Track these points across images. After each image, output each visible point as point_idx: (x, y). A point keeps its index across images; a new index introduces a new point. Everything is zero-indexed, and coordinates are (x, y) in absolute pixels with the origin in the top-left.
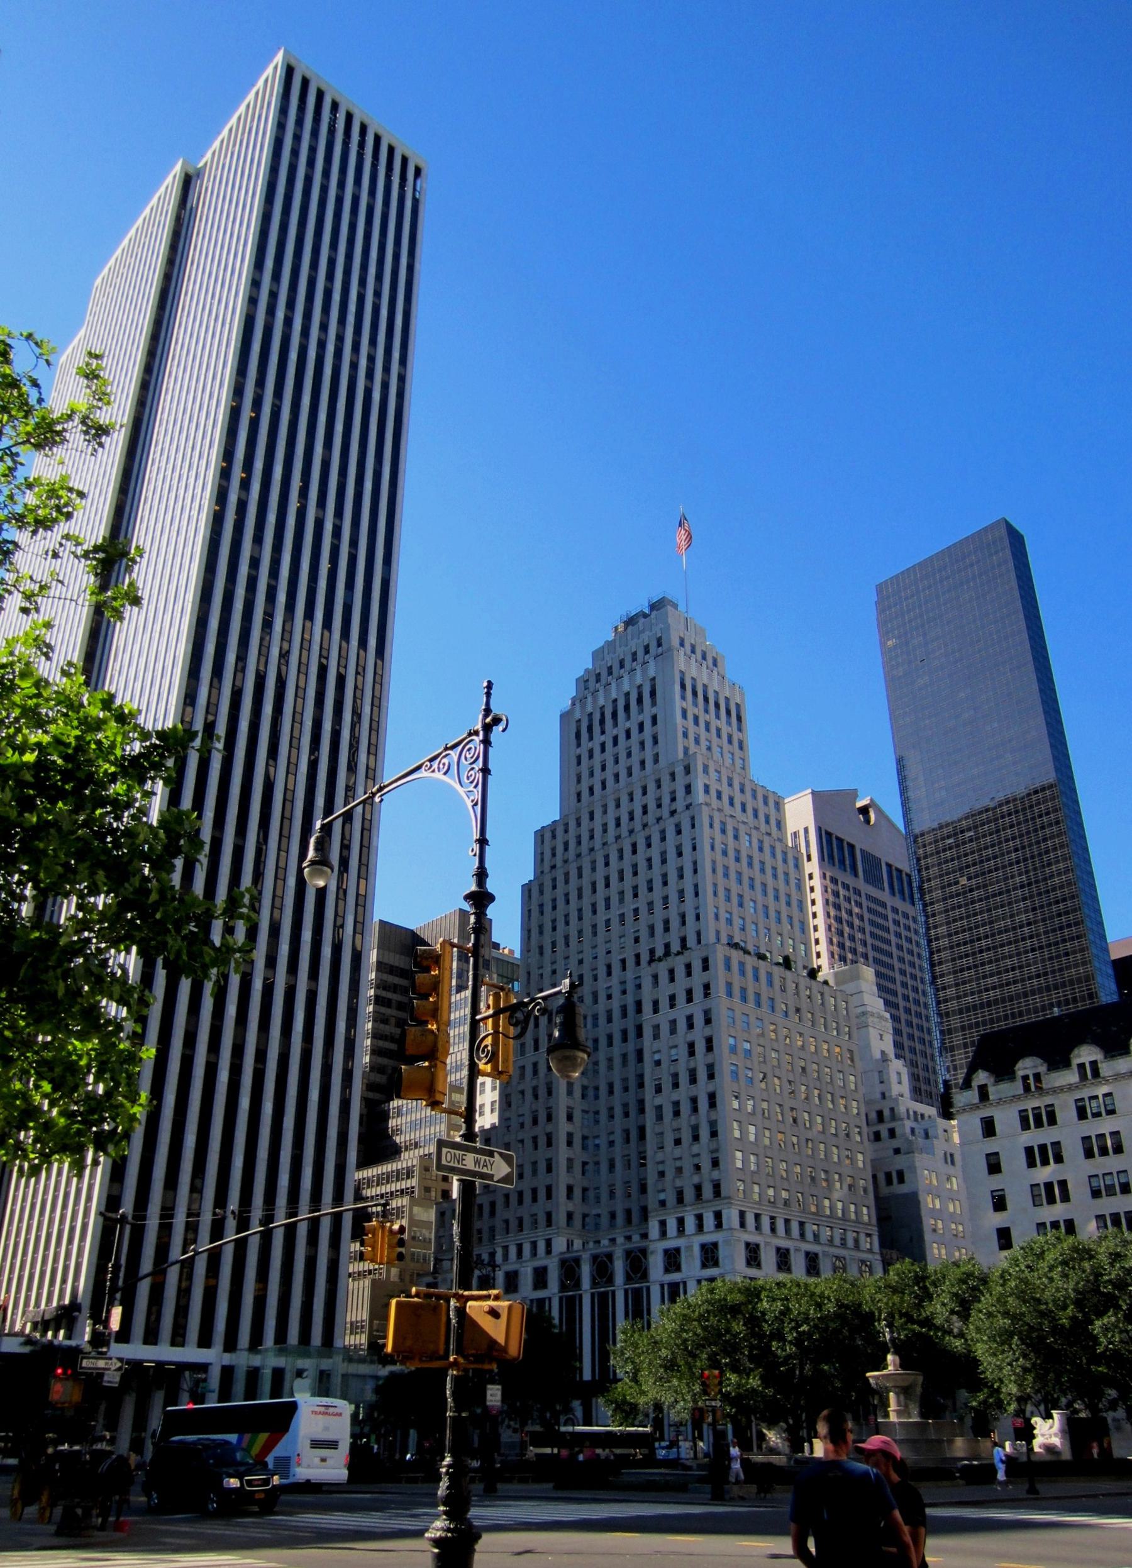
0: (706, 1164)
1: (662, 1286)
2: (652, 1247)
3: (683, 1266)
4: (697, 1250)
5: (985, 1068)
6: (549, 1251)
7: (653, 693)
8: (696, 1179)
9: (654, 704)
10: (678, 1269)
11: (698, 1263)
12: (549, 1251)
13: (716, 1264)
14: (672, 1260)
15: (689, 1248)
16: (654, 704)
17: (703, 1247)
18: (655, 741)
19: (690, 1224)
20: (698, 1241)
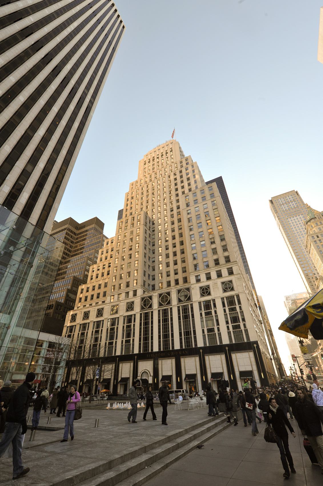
3: (212, 293)
6: (135, 294)
11: (221, 290)
12: (135, 294)
13: (232, 289)
14: (205, 291)
17: (223, 283)
19: (214, 275)
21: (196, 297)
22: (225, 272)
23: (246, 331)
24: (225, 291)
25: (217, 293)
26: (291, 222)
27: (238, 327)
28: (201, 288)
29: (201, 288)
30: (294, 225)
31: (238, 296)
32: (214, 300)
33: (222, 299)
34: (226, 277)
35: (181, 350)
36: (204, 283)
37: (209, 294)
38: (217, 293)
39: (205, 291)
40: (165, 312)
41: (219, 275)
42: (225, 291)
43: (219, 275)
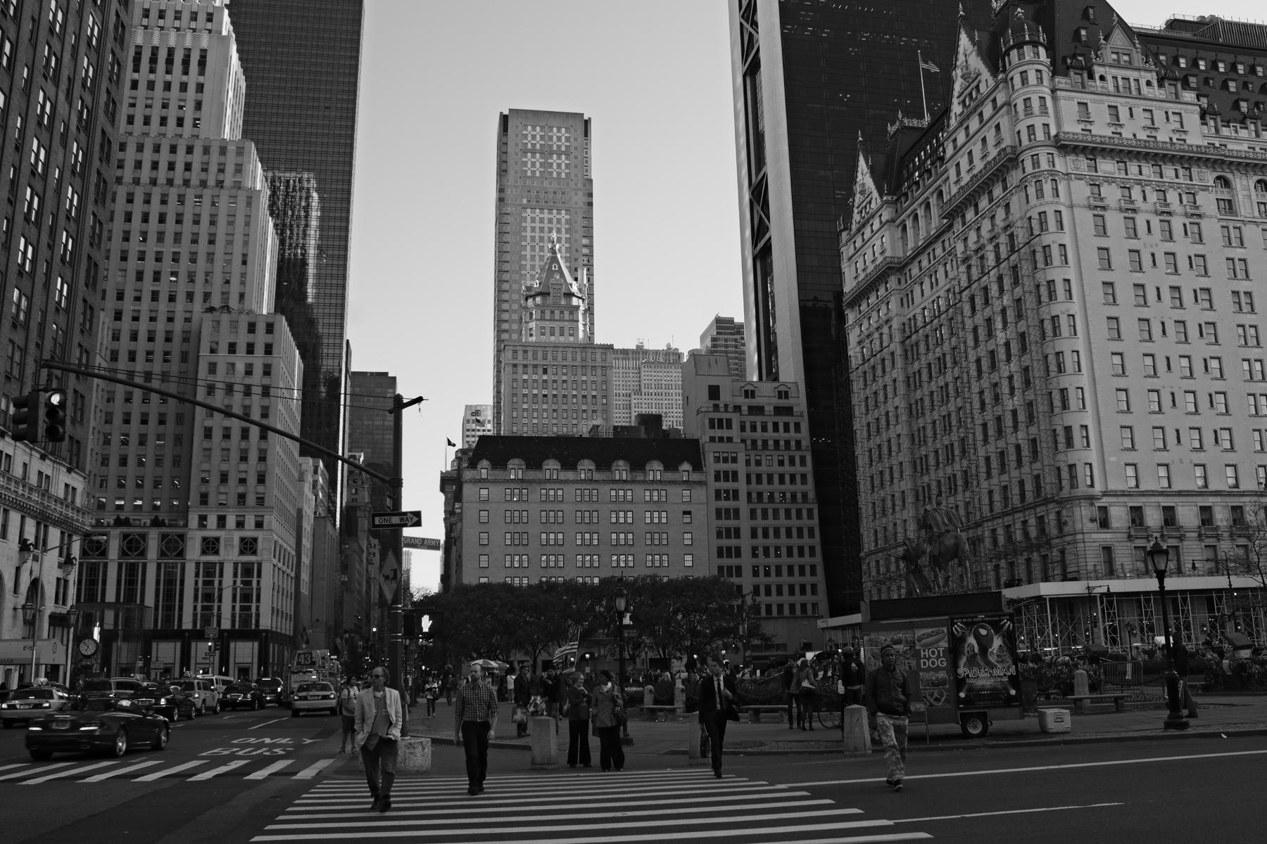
0: (252, 480)
1: (198, 564)
2: (190, 535)
3: (222, 551)
4: (236, 542)
5: (488, 459)
7: (202, 63)
8: (241, 489)
9: (202, 72)
10: (217, 553)
11: (236, 550)
13: (254, 553)
14: (210, 546)
15: (232, 539)
16: (202, 72)
17: (242, 540)
18: (198, 105)
19: (231, 521)
20: (237, 536)
21: (193, 551)
22: (250, 521)
23: (258, 615)
24: (242, 553)
25: (230, 555)
26: (528, 224)
27: (249, 608)
28: (204, 539)
29: (204, 539)
30: (533, 238)
31: (260, 565)
32: (222, 564)
33: (236, 564)
34: (249, 531)
35: (155, 630)
36: (212, 531)
37: (217, 553)
38: (230, 555)
39: (210, 546)
40: (132, 569)
41: (240, 525)
42: (242, 553)
43: (240, 525)
